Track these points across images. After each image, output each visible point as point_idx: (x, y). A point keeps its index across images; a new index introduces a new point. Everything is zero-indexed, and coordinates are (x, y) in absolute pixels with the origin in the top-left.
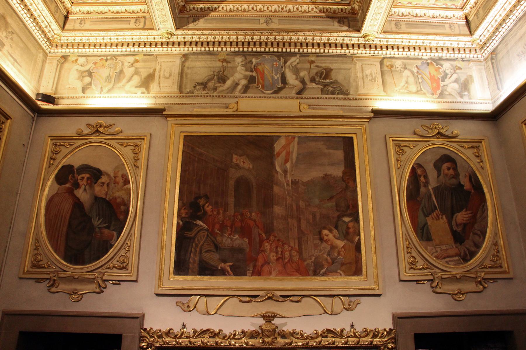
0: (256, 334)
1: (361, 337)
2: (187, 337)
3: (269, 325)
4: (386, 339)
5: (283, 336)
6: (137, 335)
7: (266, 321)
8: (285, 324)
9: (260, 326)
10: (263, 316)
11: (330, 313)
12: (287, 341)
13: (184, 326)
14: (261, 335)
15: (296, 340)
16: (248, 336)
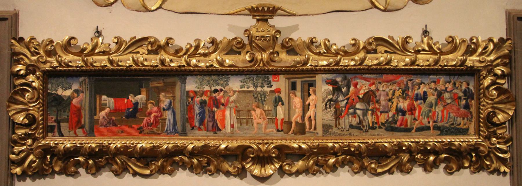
0: (238, 46)
1: (442, 53)
2: (104, 53)
3: (262, 26)
4: (492, 58)
5: (291, 51)
6: (6, 52)
7: (258, 20)
8: (295, 28)
9: (246, 31)
10: (253, 11)
11: (382, 8)
12: (298, 58)
13: (98, 33)
14: (248, 48)
15: (316, 57)
16: (223, 50)
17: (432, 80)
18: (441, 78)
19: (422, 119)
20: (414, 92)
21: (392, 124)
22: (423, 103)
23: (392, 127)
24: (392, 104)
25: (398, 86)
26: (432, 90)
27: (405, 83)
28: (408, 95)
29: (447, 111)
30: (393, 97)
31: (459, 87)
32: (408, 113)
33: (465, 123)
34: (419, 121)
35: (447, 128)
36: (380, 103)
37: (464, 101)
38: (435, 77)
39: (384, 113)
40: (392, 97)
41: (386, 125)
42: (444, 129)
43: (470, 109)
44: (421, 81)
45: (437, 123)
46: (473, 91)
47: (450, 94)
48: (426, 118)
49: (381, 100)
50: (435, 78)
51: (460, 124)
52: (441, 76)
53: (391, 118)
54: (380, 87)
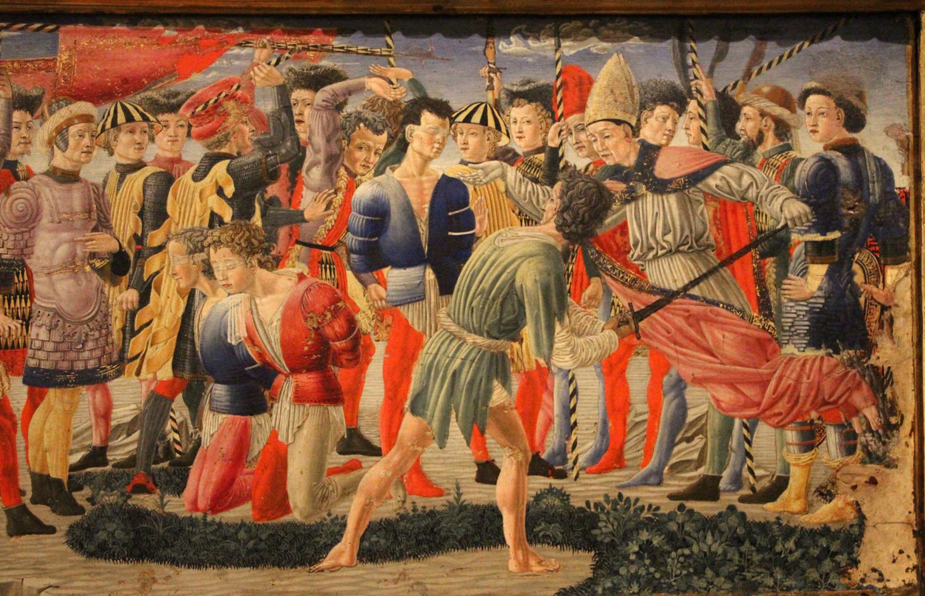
17: (513, 81)
18: (599, 59)
19: (422, 439)
20: (351, 188)
21: (141, 489)
22: (432, 292)
23: (139, 515)
24: (144, 300)
25: (200, 137)
26: (512, 173)
27: (267, 106)
28: (298, 218)
29: (660, 366)
30: (156, 238)
31: (770, 142)
32: (287, 387)
33: (820, 478)
34: (393, 456)
35: (657, 523)
36: (28, 293)
37: (818, 271)
38: (545, 45)
39: (64, 384)
40: (139, 239)
41: (80, 497)
42: (626, 537)
43: (868, 347)
44: (415, 84)
45: (562, 475)
46: (902, 181)
47: (686, 206)
48: (455, 429)
49: (32, 263)
50: (543, 62)
51: (779, 485)
52: (595, 45)
53: (130, 428)
54: (27, 142)
